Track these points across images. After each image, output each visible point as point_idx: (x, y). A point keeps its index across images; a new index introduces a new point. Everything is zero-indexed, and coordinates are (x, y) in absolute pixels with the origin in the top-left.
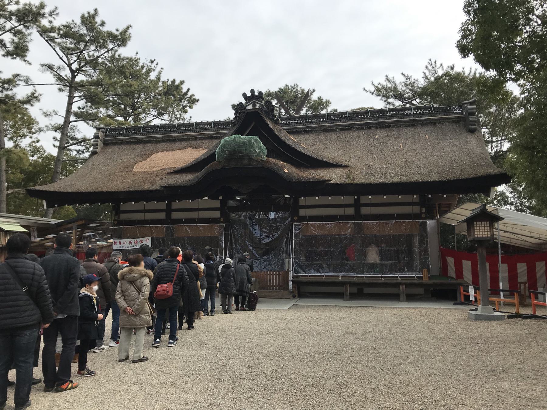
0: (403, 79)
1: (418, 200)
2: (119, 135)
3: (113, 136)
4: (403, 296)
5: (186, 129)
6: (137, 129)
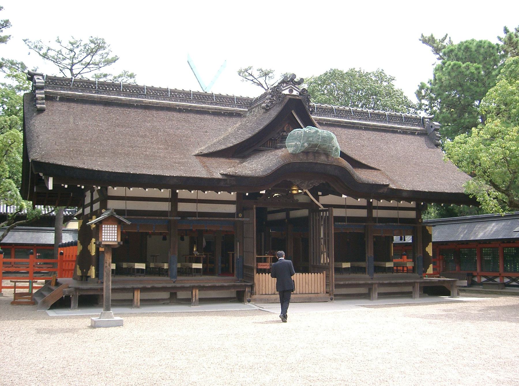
1: (414, 206)
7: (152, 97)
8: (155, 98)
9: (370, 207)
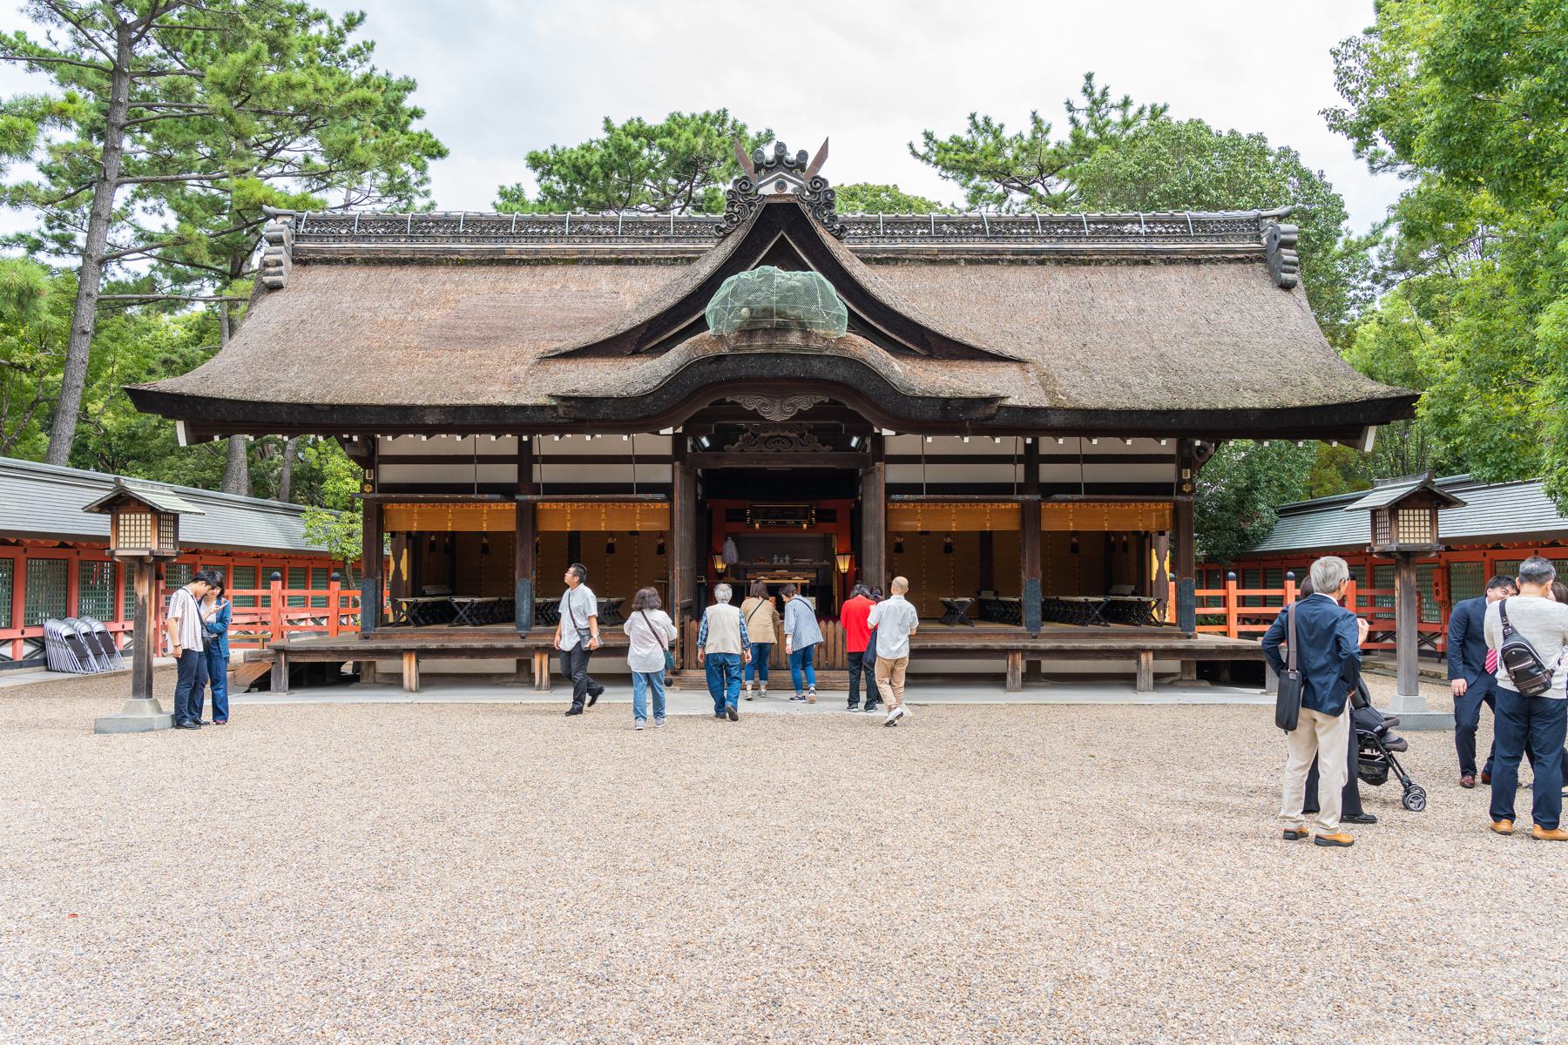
0: (1027, 129)
1: (1172, 451)
2: (338, 238)
3: (319, 238)
4: (1146, 679)
5: (541, 233)
6: (393, 225)
7: (529, 240)
8: (536, 240)
9: (1031, 459)
